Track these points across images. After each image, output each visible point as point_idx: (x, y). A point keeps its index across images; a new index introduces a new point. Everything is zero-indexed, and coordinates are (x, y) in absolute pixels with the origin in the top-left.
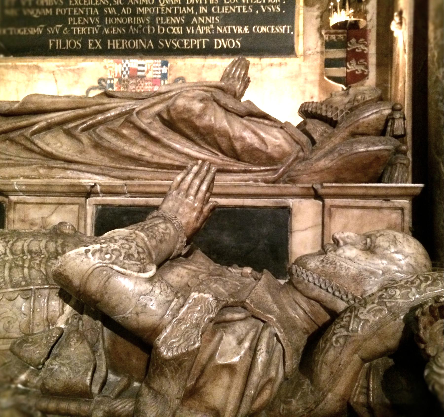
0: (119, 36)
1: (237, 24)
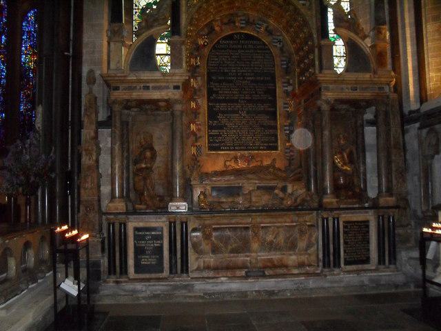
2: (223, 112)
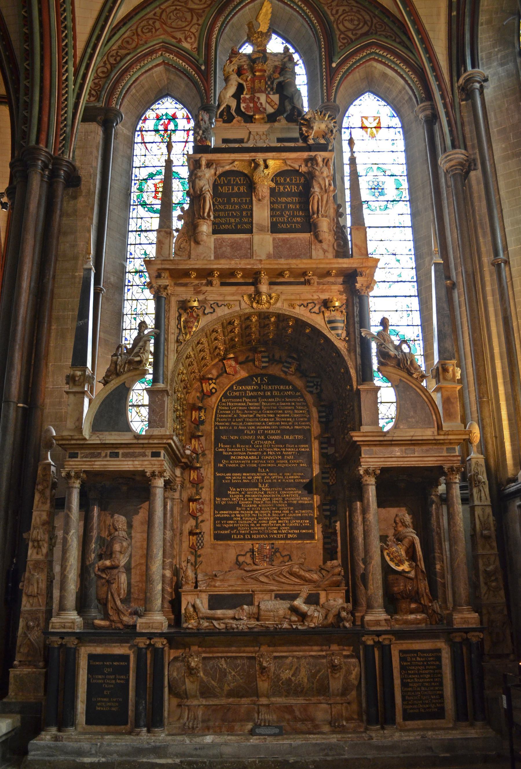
2: (236, 485)
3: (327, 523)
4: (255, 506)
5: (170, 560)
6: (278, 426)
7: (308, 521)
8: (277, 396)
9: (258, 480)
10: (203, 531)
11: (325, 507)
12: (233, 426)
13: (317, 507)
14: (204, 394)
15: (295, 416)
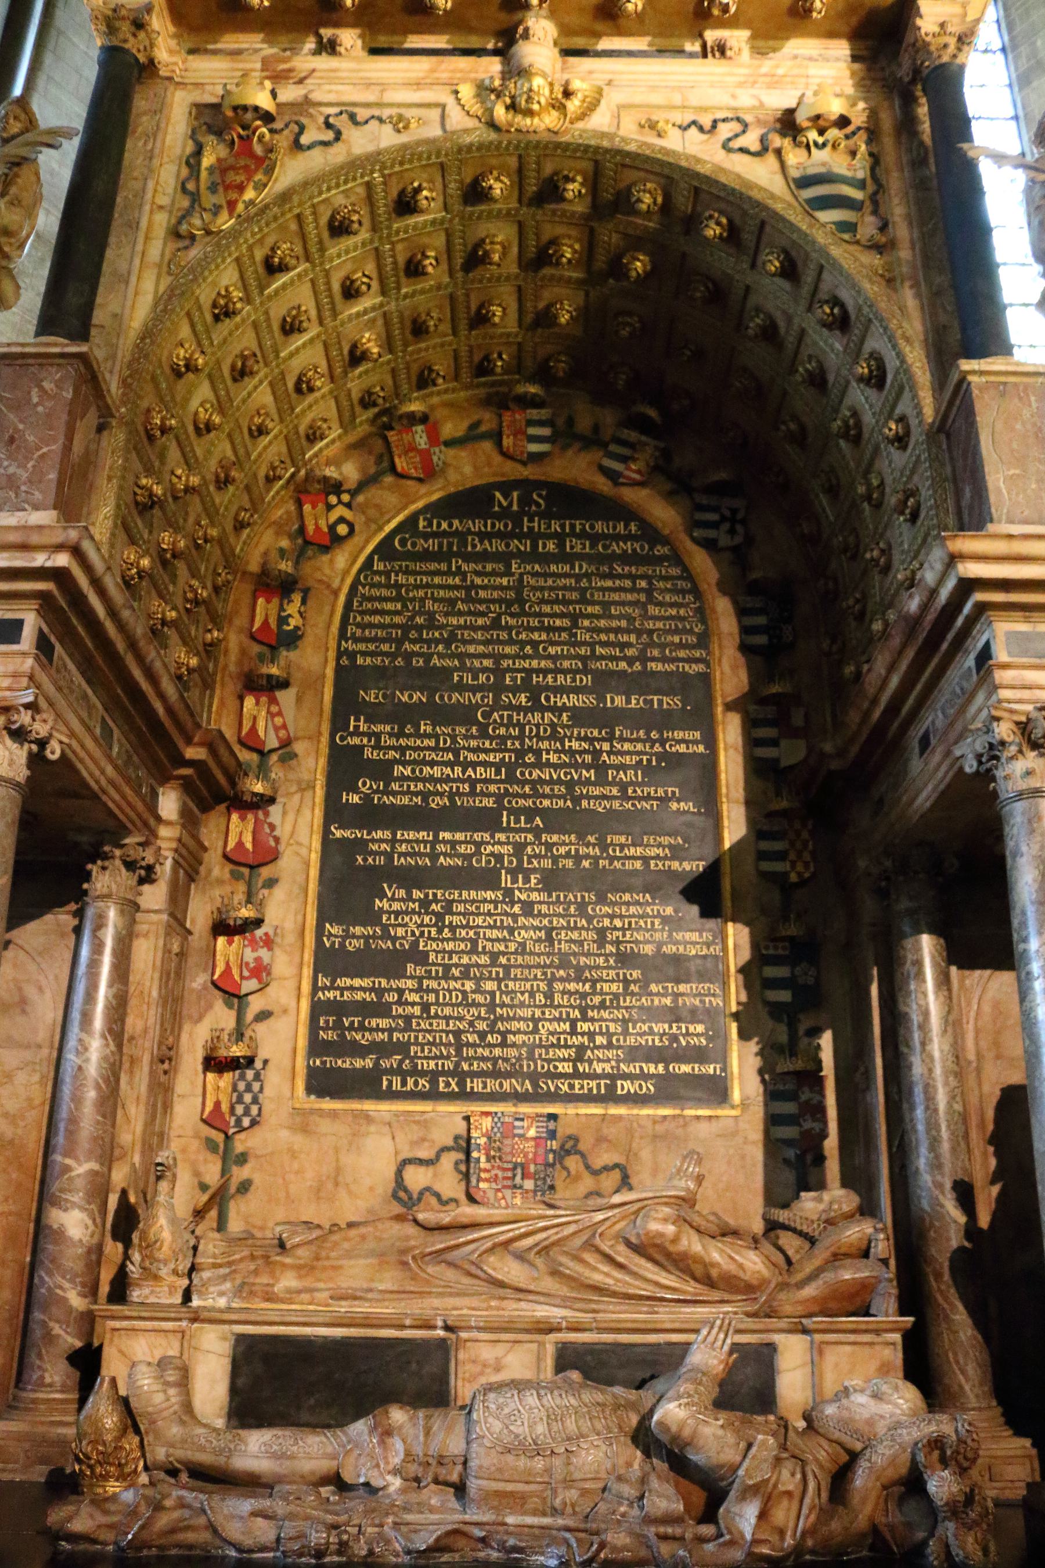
0: (481, 1074)
1: (648, 1060)
3: (783, 1038)
4: (484, 960)
5: (93, 1165)
6: (584, 659)
7: (700, 1028)
8: (581, 557)
9: (499, 858)
10: (262, 1054)
11: (770, 972)
12: (408, 656)
13: (742, 970)
14: (307, 543)
15: (650, 625)
